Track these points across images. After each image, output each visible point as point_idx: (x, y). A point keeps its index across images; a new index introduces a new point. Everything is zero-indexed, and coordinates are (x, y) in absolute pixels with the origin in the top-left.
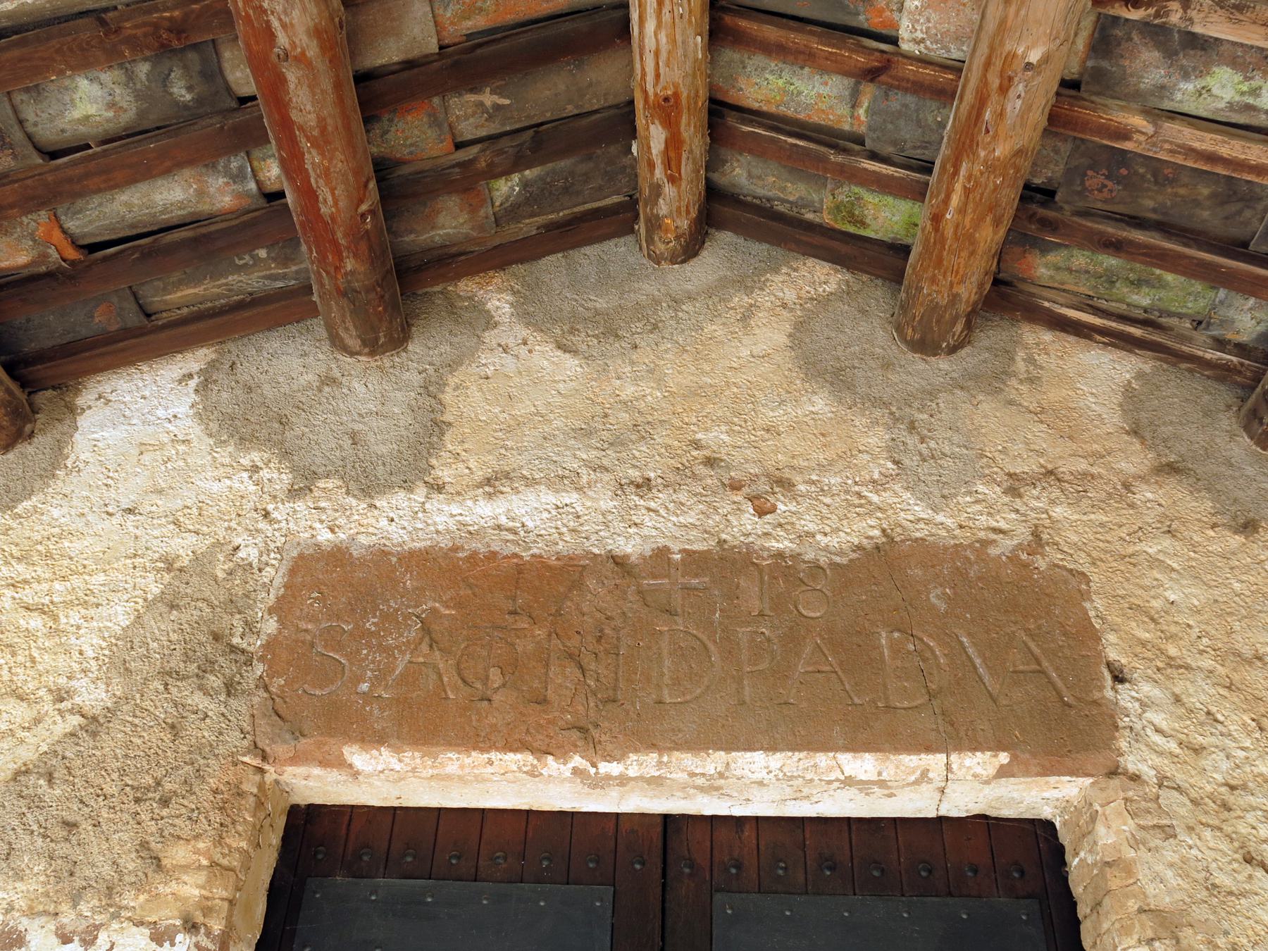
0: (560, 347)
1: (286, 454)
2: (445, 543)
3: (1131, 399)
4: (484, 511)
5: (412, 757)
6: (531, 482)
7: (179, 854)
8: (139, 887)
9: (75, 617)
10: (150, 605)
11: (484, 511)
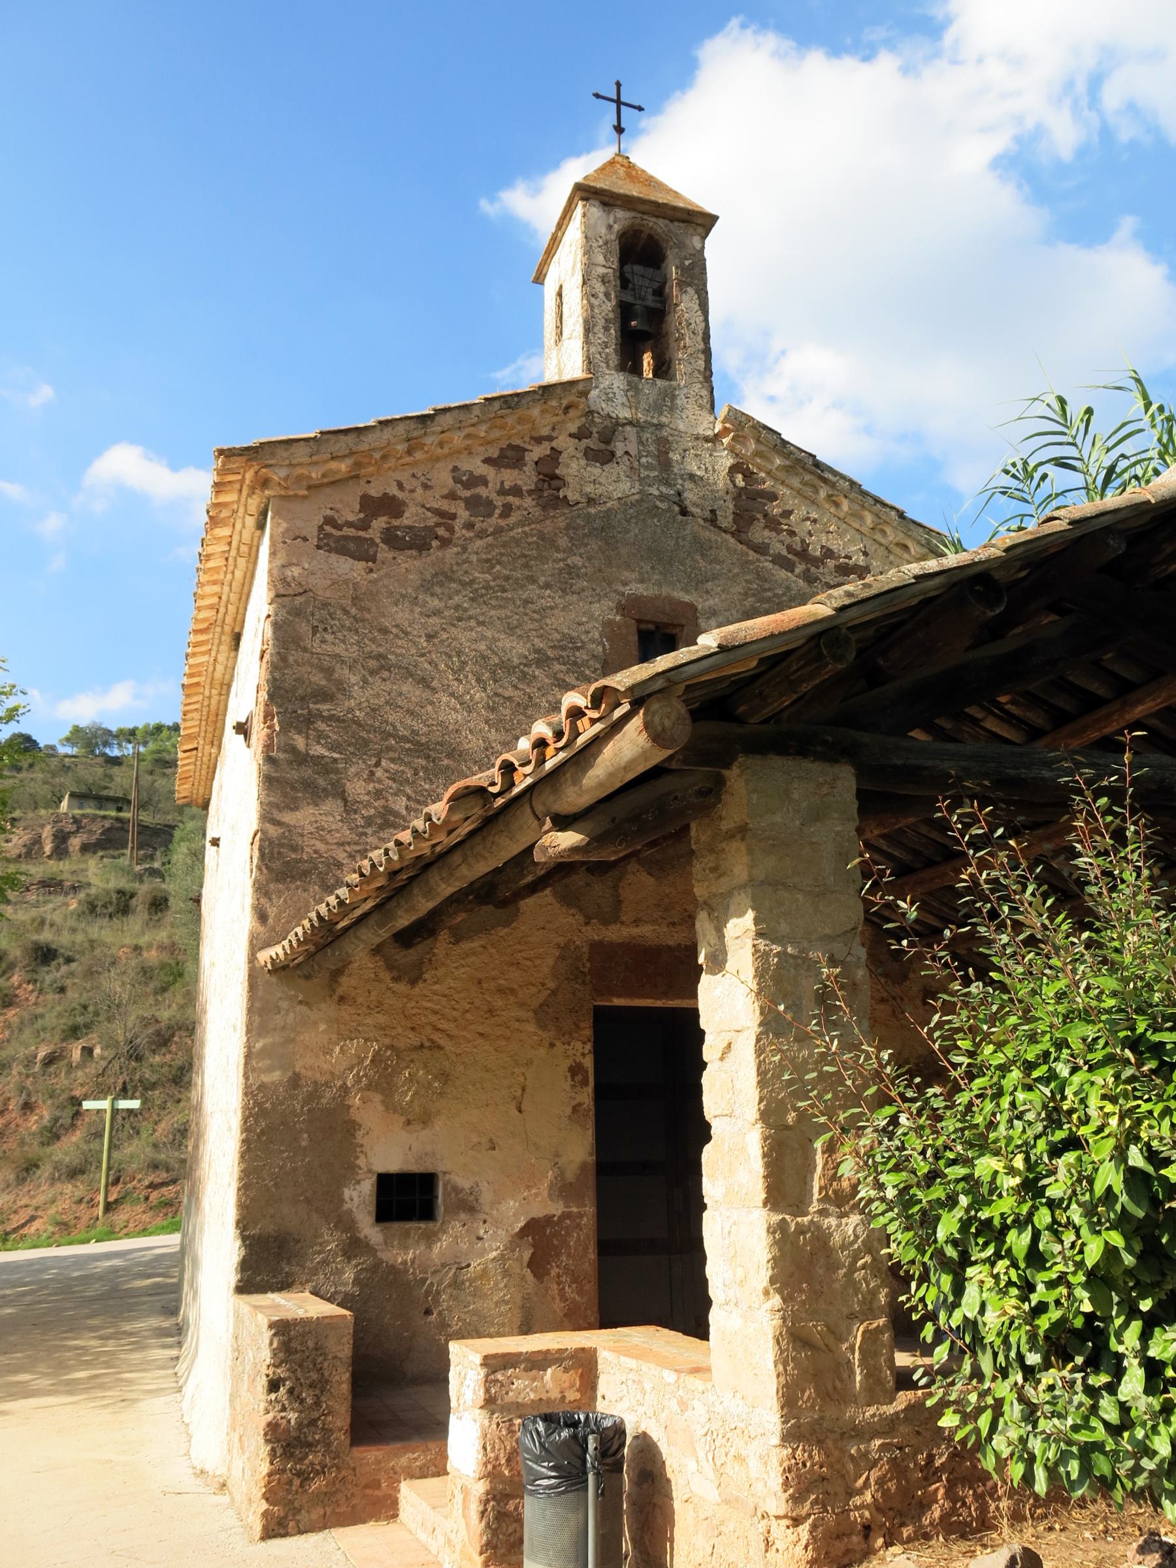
1: (581, 911)
4: (635, 931)
7: (582, 1025)
9: (538, 962)
10: (558, 958)
11: (635, 931)
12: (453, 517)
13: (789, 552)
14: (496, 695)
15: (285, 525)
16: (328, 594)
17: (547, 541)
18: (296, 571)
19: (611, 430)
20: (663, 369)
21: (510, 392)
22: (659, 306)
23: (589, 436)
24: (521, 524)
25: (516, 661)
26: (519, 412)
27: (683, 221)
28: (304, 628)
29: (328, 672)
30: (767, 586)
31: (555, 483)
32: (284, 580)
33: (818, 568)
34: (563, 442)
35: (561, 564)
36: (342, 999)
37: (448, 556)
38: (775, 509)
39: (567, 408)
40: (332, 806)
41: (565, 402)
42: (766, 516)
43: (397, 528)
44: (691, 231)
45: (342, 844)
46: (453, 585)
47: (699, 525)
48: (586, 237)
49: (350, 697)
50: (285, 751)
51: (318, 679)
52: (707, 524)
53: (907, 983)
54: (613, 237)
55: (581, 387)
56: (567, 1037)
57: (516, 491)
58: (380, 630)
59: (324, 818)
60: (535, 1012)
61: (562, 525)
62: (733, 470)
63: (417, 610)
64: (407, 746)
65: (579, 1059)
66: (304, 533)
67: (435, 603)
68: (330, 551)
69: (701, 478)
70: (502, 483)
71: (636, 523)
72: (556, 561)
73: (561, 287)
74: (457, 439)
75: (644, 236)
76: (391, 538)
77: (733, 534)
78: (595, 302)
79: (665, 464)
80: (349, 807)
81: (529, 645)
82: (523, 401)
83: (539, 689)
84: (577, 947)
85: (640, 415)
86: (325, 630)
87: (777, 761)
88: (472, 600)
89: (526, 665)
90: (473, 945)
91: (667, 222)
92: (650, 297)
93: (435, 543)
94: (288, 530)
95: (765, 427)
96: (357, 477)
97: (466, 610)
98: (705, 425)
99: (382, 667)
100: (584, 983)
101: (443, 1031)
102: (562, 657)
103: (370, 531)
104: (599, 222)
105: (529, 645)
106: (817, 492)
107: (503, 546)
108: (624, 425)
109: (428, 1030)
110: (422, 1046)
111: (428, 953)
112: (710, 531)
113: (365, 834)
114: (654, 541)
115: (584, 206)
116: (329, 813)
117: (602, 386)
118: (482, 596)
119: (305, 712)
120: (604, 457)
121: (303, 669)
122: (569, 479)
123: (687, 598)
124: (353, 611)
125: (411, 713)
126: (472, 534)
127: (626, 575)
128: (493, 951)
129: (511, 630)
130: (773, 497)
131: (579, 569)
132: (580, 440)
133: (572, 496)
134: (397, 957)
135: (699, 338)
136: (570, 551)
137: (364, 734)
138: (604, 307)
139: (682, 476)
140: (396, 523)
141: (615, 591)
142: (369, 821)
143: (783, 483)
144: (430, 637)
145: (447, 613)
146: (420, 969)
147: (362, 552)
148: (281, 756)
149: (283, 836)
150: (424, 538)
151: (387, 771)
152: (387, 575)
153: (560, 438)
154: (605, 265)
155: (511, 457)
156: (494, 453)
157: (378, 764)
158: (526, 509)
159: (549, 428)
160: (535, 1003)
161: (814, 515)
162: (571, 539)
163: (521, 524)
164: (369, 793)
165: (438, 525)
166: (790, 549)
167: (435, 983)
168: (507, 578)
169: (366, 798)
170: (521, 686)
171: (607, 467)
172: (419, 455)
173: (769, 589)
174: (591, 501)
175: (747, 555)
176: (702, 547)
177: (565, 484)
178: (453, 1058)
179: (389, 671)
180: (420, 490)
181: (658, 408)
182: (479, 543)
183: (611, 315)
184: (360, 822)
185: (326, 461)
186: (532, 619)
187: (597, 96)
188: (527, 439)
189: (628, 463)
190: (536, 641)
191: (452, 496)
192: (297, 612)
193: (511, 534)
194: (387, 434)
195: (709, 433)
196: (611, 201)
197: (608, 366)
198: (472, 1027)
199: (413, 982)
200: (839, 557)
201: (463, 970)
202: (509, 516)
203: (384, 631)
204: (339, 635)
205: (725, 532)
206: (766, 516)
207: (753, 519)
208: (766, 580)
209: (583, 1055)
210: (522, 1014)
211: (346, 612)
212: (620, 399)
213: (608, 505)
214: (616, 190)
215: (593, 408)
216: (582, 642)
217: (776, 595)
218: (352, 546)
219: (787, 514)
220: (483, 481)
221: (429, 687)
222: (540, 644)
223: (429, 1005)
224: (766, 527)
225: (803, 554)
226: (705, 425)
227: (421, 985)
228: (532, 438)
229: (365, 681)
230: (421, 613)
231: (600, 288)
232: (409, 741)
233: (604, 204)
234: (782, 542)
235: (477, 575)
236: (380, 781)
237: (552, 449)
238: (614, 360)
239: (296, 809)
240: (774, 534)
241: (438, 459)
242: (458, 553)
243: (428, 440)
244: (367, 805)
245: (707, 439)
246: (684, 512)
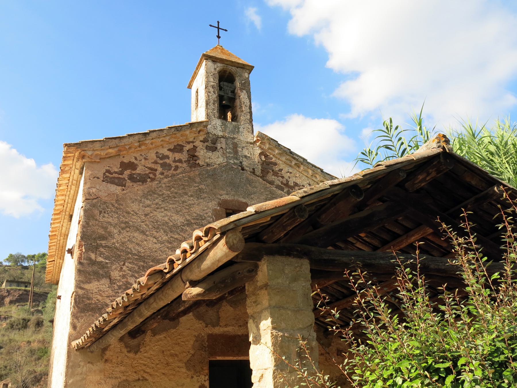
0: (231, 306)
1: (204, 321)
4: (226, 329)
5: (223, 357)
6: (230, 326)
7: (204, 368)
8: (202, 371)
9: (187, 343)
11: (226, 329)
12: (156, 170)
13: (282, 184)
14: (172, 237)
15: (90, 173)
16: (106, 199)
17: (192, 180)
18: (94, 190)
19: (215, 140)
20: (234, 118)
21: (178, 125)
22: (233, 96)
23: (208, 141)
24: (182, 173)
25: (179, 224)
26: (181, 133)
27: (242, 68)
28: (96, 212)
29: (105, 228)
31: (195, 158)
32: (89, 194)
33: (292, 190)
34: (198, 143)
35: (197, 188)
36: (106, 361)
37: (153, 185)
39: (200, 131)
40: (105, 281)
41: (199, 129)
42: (273, 171)
43: (134, 174)
44: (244, 71)
45: (108, 297)
46: (156, 196)
47: (249, 174)
48: (207, 72)
49: (114, 238)
50: (87, 260)
51: (101, 231)
52: (251, 174)
53: (331, 347)
54: (216, 72)
55: (204, 124)
56: (198, 374)
57: (180, 161)
58: (126, 213)
59: (101, 286)
60: (186, 364)
61: (197, 173)
62: (261, 154)
63: (141, 205)
64: (136, 257)
65: (203, 382)
66: (98, 176)
67: (148, 202)
68: (107, 183)
69: (249, 157)
70: (175, 158)
72: (195, 187)
73: (197, 89)
74: (158, 141)
75: (228, 72)
76: (131, 178)
77: (261, 177)
78: (210, 95)
79: (236, 152)
80: (112, 281)
81: (184, 218)
82: (183, 129)
83: (188, 235)
84: (203, 336)
85: (226, 134)
86: (105, 212)
87: (279, 258)
88: (163, 201)
89: (183, 226)
90: (160, 337)
91: (235, 68)
92: (230, 93)
93: (149, 180)
94: (91, 174)
95: (272, 139)
96: (119, 155)
97: (160, 205)
99: (127, 227)
100: (205, 351)
101: (148, 373)
102: (197, 223)
103: (124, 175)
104: (211, 67)
105: (184, 218)
106: (291, 162)
107: (175, 181)
108: (220, 138)
109: (142, 372)
110: (139, 379)
111: (142, 340)
112: (253, 176)
113: (118, 292)
114: (232, 180)
115: (206, 62)
116: (103, 285)
117: (212, 124)
118: (166, 200)
119: (95, 244)
120: (213, 149)
121: (95, 228)
122: (200, 157)
123: (244, 201)
124: (116, 205)
125: (138, 244)
126: (163, 177)
127: (222, 192)
128: (169, 339)
129: (177, 212)
130: (275, 164)
131: (204, 190)
132: (204, 143)
133: (201, 163)
134: (130, 342)
135: (248, 108)
136: (200, 183)
137: (119, 253)
138: (213, 96)
139: (242, 156)
140: (134, 172)
141: (217, 198)
142: (120, 287)
143: (279, 159)
144: (146, 215)
145: (153, 206)
146: (139, 347)
147: (120, 183)
148: (85, 261)
149: (84, 294)
150: (145, 178)
151: (128, 267)
152: (130, 192)
153: (197, 142)
154: (214, 82)
155: (178, 149)
157: (124, 265)
158: (183, 168)
159: (193, 138)
160: (185, 360)
161: (290, 171)
162: (201, 179)
163: (182, 173)
164: (120, 276)
165: (150, 173)
166: (282, 183)
167: (145, 353)
168: (176, 193)
169: (119, 278)
170: (181, 234)
171: (214, 153)
172: (143, 147)
174: (208, 165)
175: (267, 185)
176: (250, 182)
177: (198, 158)
178: (152, 384)
179: (129, 228)
180: (143, 160)
181: (233, 132)
182: (166, 180)
183: (216, 99)
184: (116, 287)
185: (107, 149)
186: (186, 208)
187: (211, 26)
188: (184, 142)
189: (222, 151)
190: (187, 217)
191: (155, 162)
192: (94, 206)
193: (178, 177)
194: (131, 139)
195: (252, 141)
196: (216, 60)
197: (215, 117)
198: (160, 371)
199: (136, 353)
200: (300, 186)
201: (156, 347)
202: (177, 170)
203: (128, 213)
204: (110, 214)
205: (258, 176)
206: (273, 171)
207: (268, 172)
208: (273, 194)
209: (205, 381)
210: (180, 364)
211: (113, 206)
212: (219, 128)
213: (215, 166)
214: (217, 56)
215: (209, 131)
216: (205, 217)
218: (116, 181)
219: (281, 170)
220: (168, 157)
221: (145, 234)
222: (188, 218)
223: (142, 362)
224: (273, 175)
225: (287, 185)
226: (250, 138)
227: (139, 353)
228: (186, 142)
229: (120, 232)
230: (143, 206)
231: (211, 90)
232: (137, 255)
233: (213, 61)
235: (165, 192)
236: (124, 271)
237: (194, 146)
238: (217, 115)
239: (90, 283)
240: (276, 177)
241: (150, 149)
242: (158, 184)
243: (147, 142)
244: (119, 281)
245: (251, 143)
246: (243, 169)
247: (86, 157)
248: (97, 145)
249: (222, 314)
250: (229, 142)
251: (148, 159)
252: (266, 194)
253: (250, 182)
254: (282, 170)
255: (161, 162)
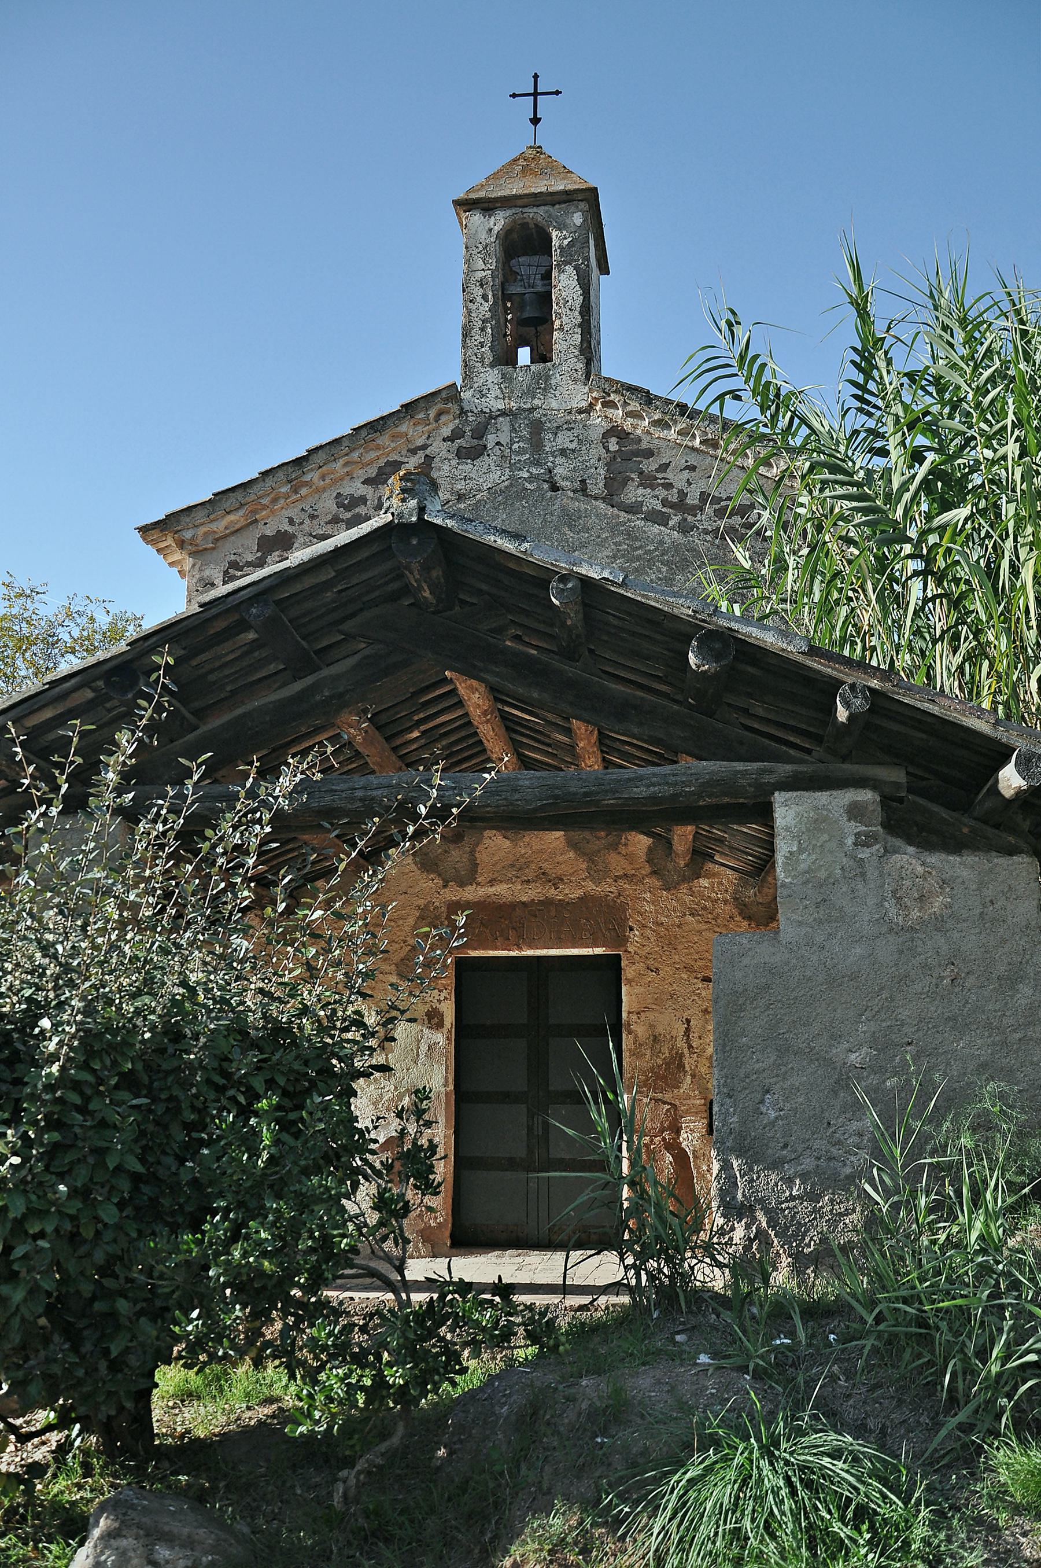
1: (439, 875)
2: (482, 899)
3: (650, 849)
4: (492, 890)
9: (401, 922)
11: (492, 890)
13: (664, 506)
27: (565, 202)
30: (638, 544)
34: (438, 448)
38: (650, 466)
39: (439, 415)
41: (432, 413)
42: (641, 473)
44: (572, 209)
55: (444, 395)
62: (607, 435)
65: (436, 1005)
69: (574, 451)
71: (505, 509)
75: (532, 226)
79: (536, 444)
92: (539, 283)
96: (256, 521)
98: (579, 397)
104: (480, 229)
130: (649, 453)
132: (453, 441)
135: (577, 313)
156: (372, 472)
166: (665, 503)
172: (304, 491)
173: (641, 547)
174: (461, 497)
175: (618, 516)
176: (570, 519)
180: (307, 522)
183: (488, 315)
187: (514, 96)
188: (404, 452)
194: (269, 482)
195: (584, 404)
196: (491, 205)
205: (596, 499)
207: (626, 480)
208: (637, 539)
209: (439, 1001)
212: (495, 392)
217: (647, 552)
219: (664, 467)
224: (640, 485)
225: (680, 505)
234: (657, 497)
237: (427, 456)
238: (489, 358)
240: (649, 490)
241: (324, 490)
243: (307, 478)
245: (580, 411)
246: (555, 488)
247: (186, 545)
248: (200, 516)
249: (483, 856)
250: (522, 424)
251: (318, 516)
252: (615, 544)
253: (570, 519)
254: (668, 465)
255: (348, 515)
